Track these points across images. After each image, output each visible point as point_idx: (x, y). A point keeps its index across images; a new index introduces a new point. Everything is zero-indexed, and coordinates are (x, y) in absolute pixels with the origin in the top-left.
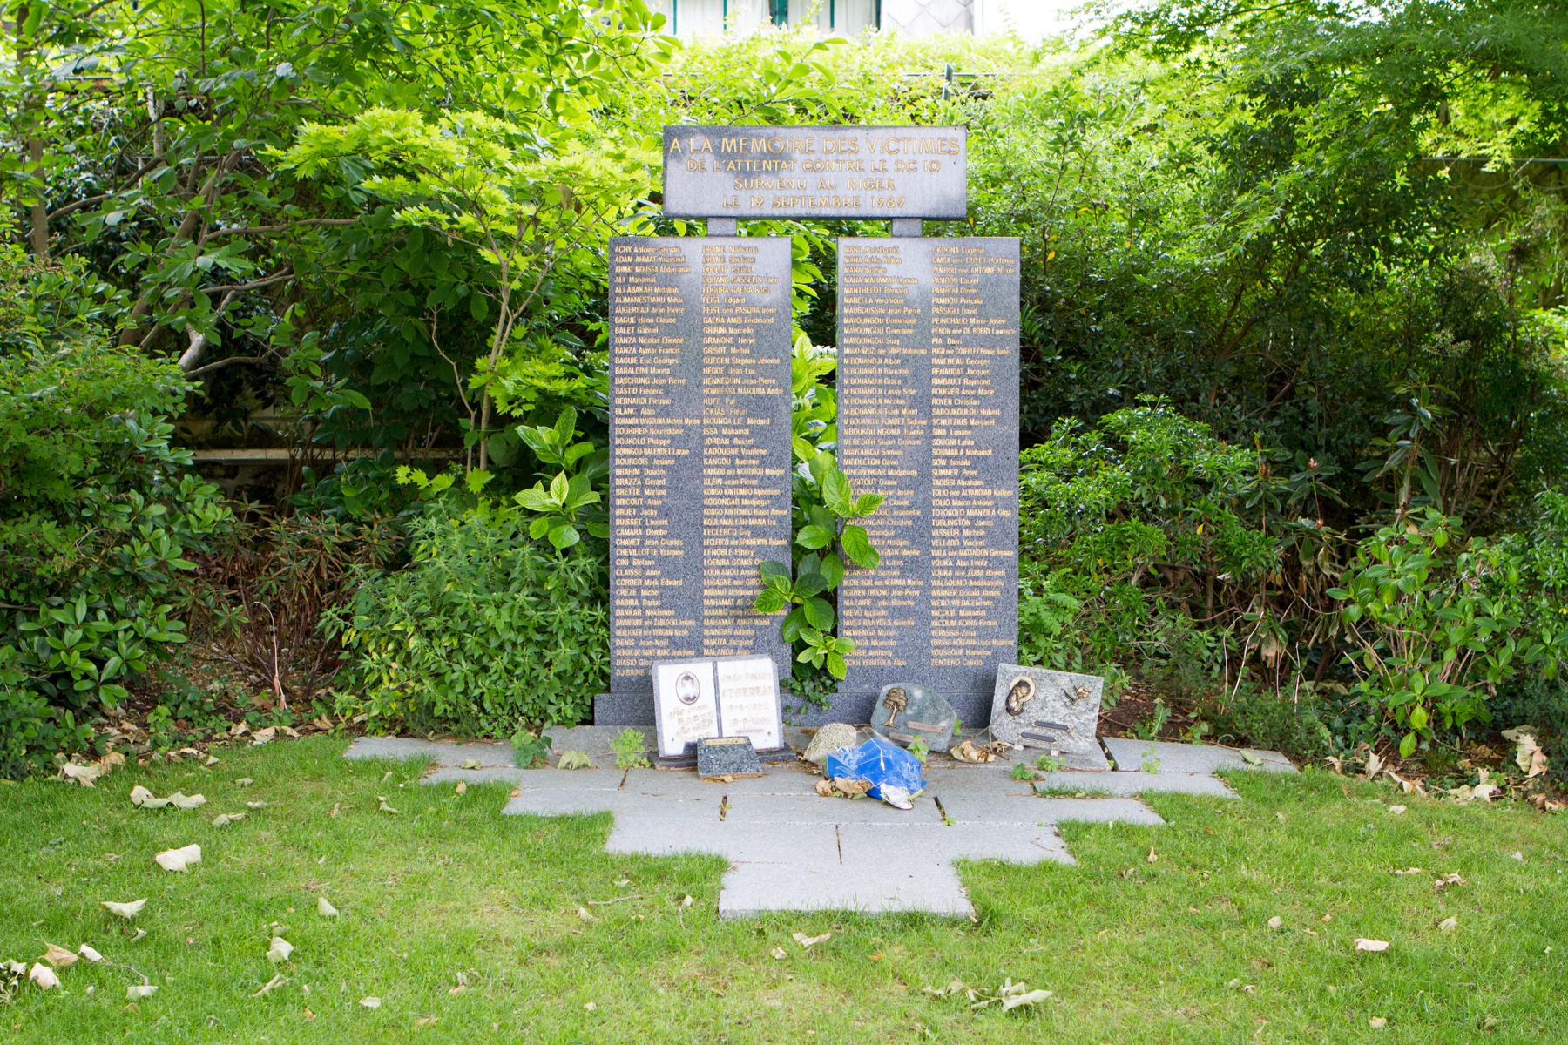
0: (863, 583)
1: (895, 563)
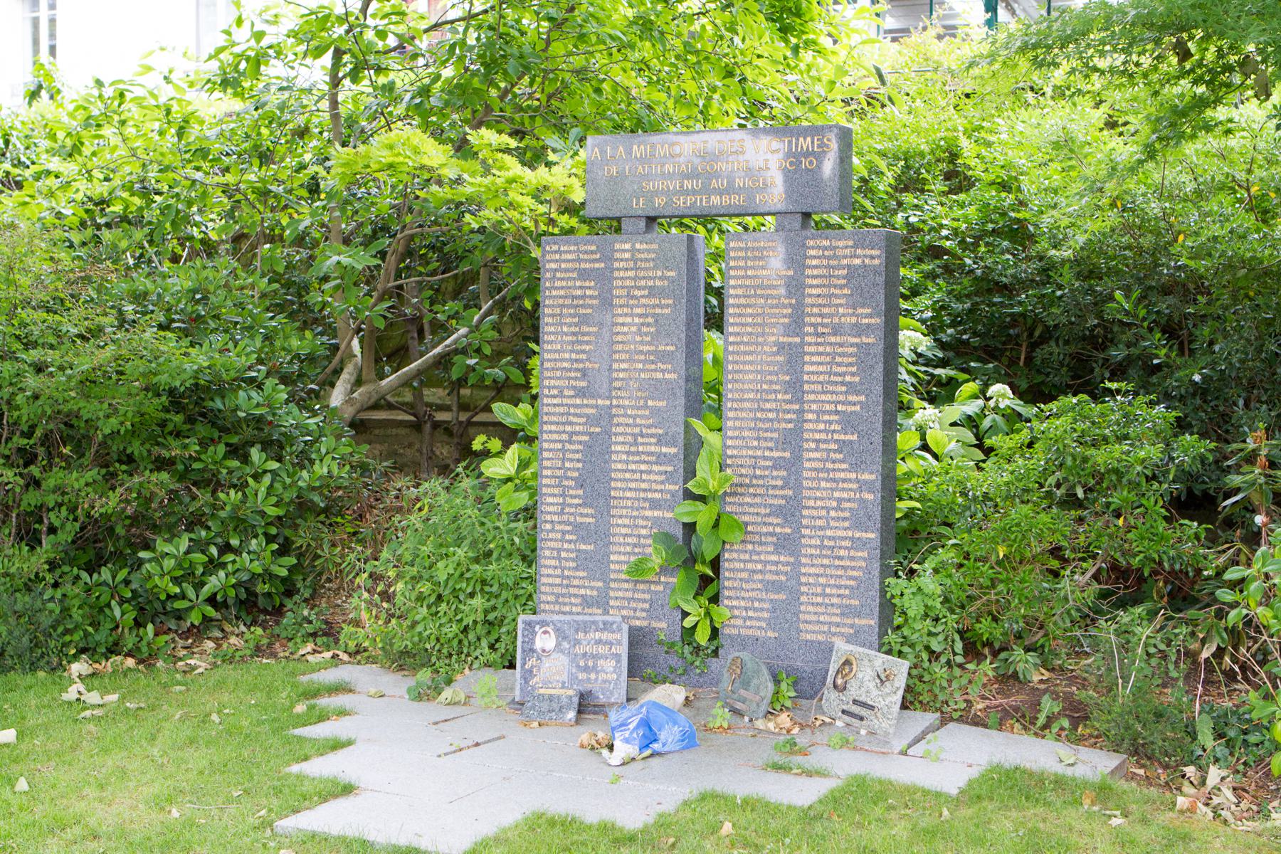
0: (742, 557)
1: (770, 539)
